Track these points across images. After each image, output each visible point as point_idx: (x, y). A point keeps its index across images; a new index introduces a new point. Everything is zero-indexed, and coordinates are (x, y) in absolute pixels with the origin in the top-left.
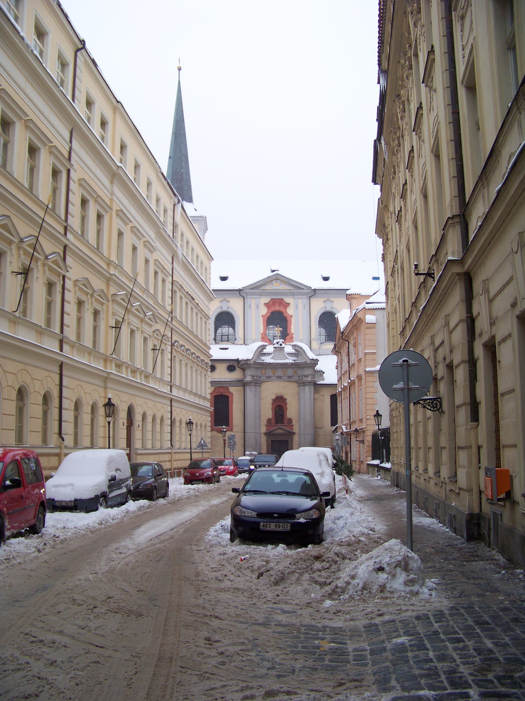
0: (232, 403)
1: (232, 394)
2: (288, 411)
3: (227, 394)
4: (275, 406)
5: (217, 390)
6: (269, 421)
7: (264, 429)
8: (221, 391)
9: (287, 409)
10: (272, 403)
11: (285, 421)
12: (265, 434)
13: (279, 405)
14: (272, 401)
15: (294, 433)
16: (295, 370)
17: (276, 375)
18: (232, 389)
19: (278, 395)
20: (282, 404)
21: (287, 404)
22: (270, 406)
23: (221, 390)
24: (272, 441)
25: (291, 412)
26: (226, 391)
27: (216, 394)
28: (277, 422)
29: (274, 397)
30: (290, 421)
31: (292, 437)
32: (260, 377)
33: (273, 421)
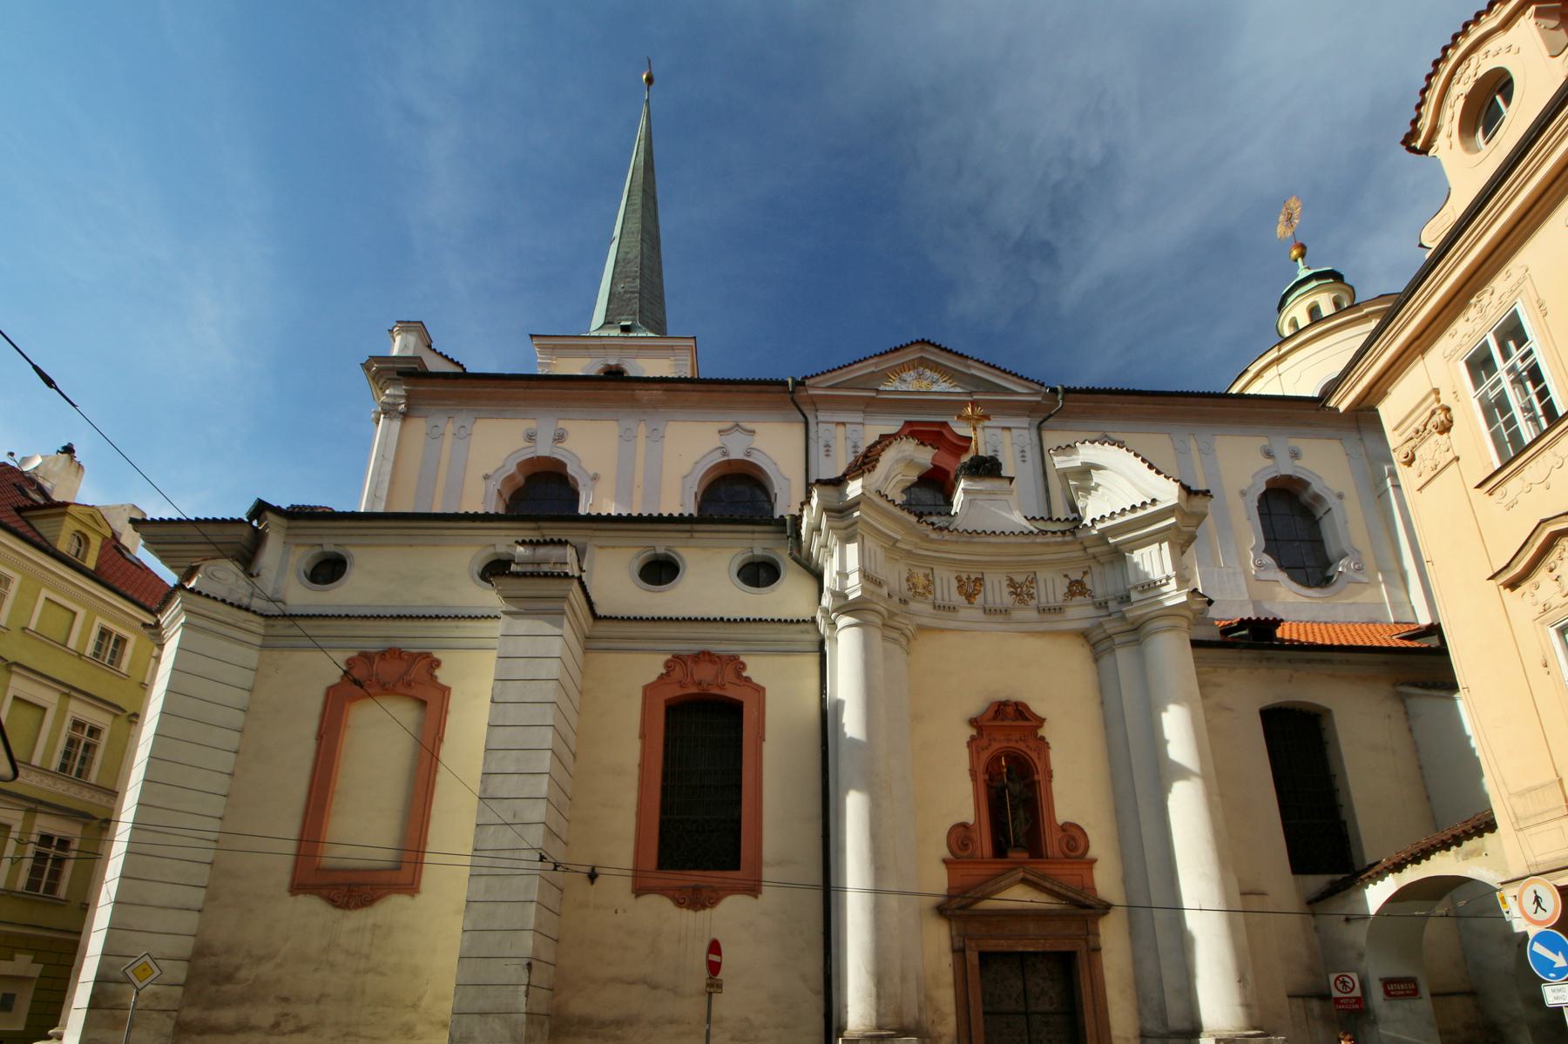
0: (760, 737)
1: (760, 690)
2: (1057, 785)
3: (732, 692)
4: (985, 756)
5: (678, 673)
6: (960, 836)
10: (971, 742)
11: (1052, 843)
15: (1107, 907)
18: (757, 668)
19: (1002, 697)
20: (1022, 746)
21: (1043, 744)
22: (963, 756)
23: (705, 673)
25: (1075, 794)
26: (729, 674)
27: (674, 692)
28: (1000, 851)
29: (975, 705)
30: (1074, 837)
31: (1097, 935)
32: (904, 602)
33: (984, 843)
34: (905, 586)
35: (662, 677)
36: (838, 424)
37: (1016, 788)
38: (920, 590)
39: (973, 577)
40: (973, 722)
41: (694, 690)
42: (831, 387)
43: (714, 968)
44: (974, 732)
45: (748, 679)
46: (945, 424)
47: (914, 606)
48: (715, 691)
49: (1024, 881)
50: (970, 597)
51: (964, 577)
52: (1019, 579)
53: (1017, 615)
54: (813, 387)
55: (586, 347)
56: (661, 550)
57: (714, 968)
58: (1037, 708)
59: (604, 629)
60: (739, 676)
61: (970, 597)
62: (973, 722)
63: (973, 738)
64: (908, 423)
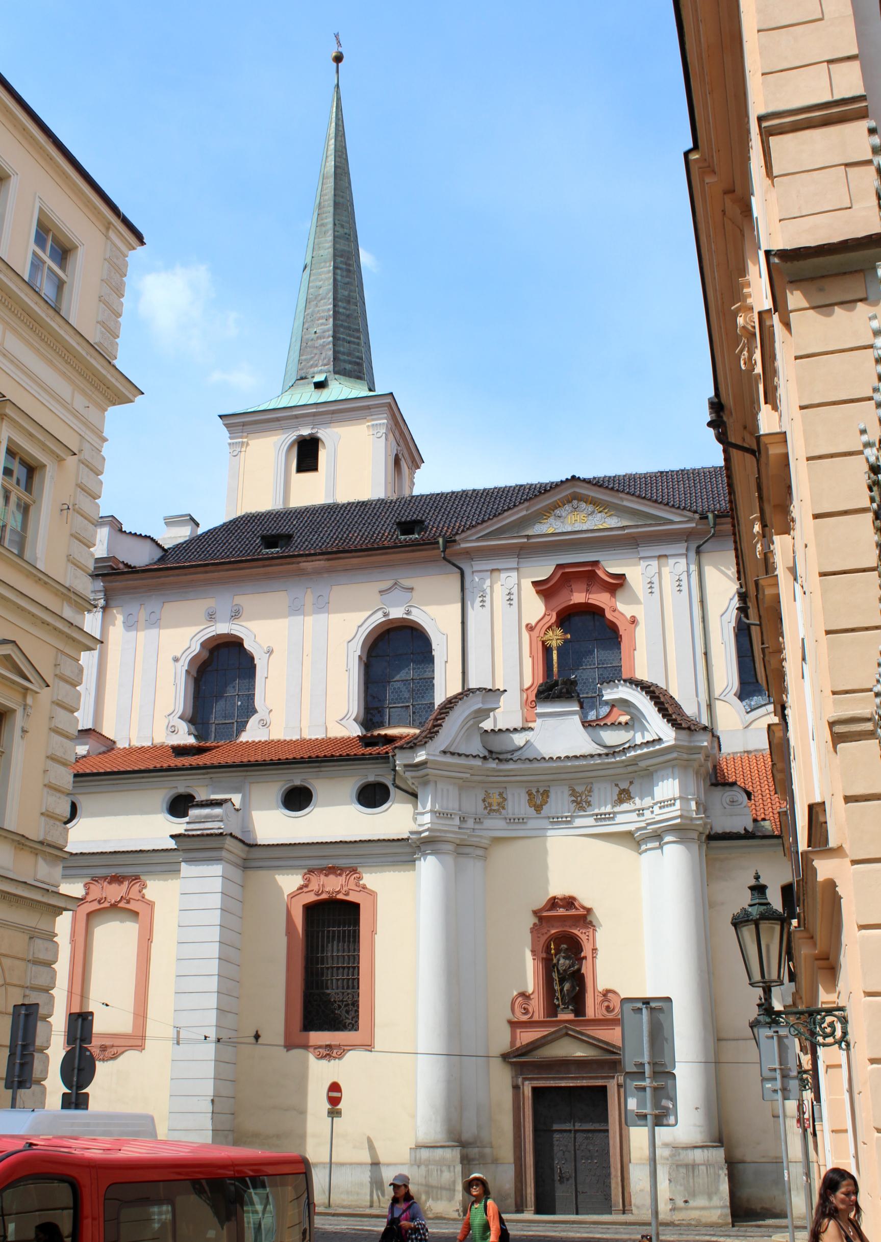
0: (373, 932)
1: (373, 894)
3: (352, 898)
4: (543, 939)
5: (314, 886)
7: (502, 1040)
8: (333, 886)
9: (595, 950)
10: (534, 930)
12: (505, 1057)
13: (563, 936)
14: (532, 920)
16: (624, 785)
17: (546, 810)
24: (537, 1092)
27: (311, 898)
28: (552, 1009)
34: (481, 805)
35: (300, 888)
36: (493, 571)
37: (563, 963)
38: (495, 807)
39: (541, 791)
40: (535, 913)
41: (324, 896)
42: (478, 540)
43: (334, 1101)
44: (536, 920)
45: (364, 887)
46: (596, 563)
47: (488, 823)
48: (340, 896)
49: (567, 1035)
50: (538, 808)
51: (534, 791)
52: (580, 789)
53: (578, 822)
54: (465, 540)
55: (278, 420)
56: (297, 783)
57: (334, 1101)
58: (585, 898)
59: (256, 853)
60: (357, 885)
61: (538, 808)
62: (535, 913)
63: (535, 924)
64: (559, 566)
